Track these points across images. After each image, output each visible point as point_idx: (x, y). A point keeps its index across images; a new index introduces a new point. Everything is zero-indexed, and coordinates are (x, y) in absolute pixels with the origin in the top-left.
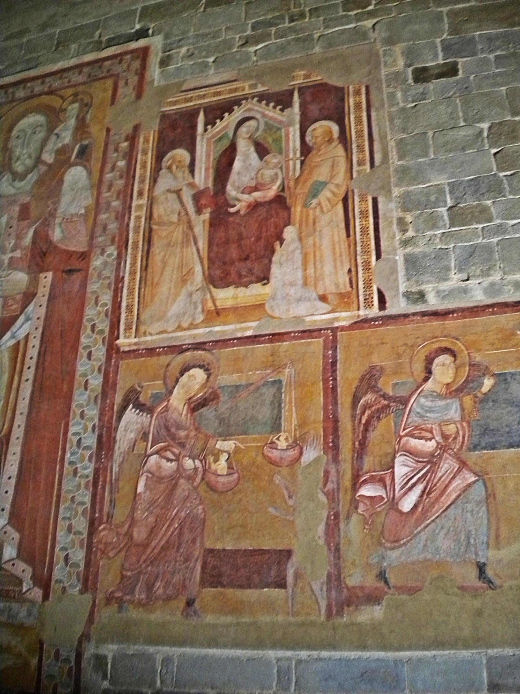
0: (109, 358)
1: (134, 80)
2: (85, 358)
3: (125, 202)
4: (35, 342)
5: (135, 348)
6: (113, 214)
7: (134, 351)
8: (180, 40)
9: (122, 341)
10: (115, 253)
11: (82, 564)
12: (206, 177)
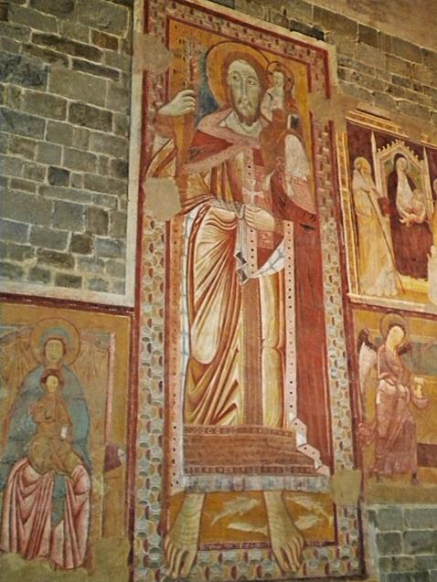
0: (344, 305)
1: (322, 77)
2: (329, 301)
3: (334, 185)
4: (290, 277)
5: (359, 302)
6: (328, 191)
7: (360, 304)
8: (348, 60)
9: (350, 294)
10: (335, 224)
11: (351, 449)
12: (383, 191)
